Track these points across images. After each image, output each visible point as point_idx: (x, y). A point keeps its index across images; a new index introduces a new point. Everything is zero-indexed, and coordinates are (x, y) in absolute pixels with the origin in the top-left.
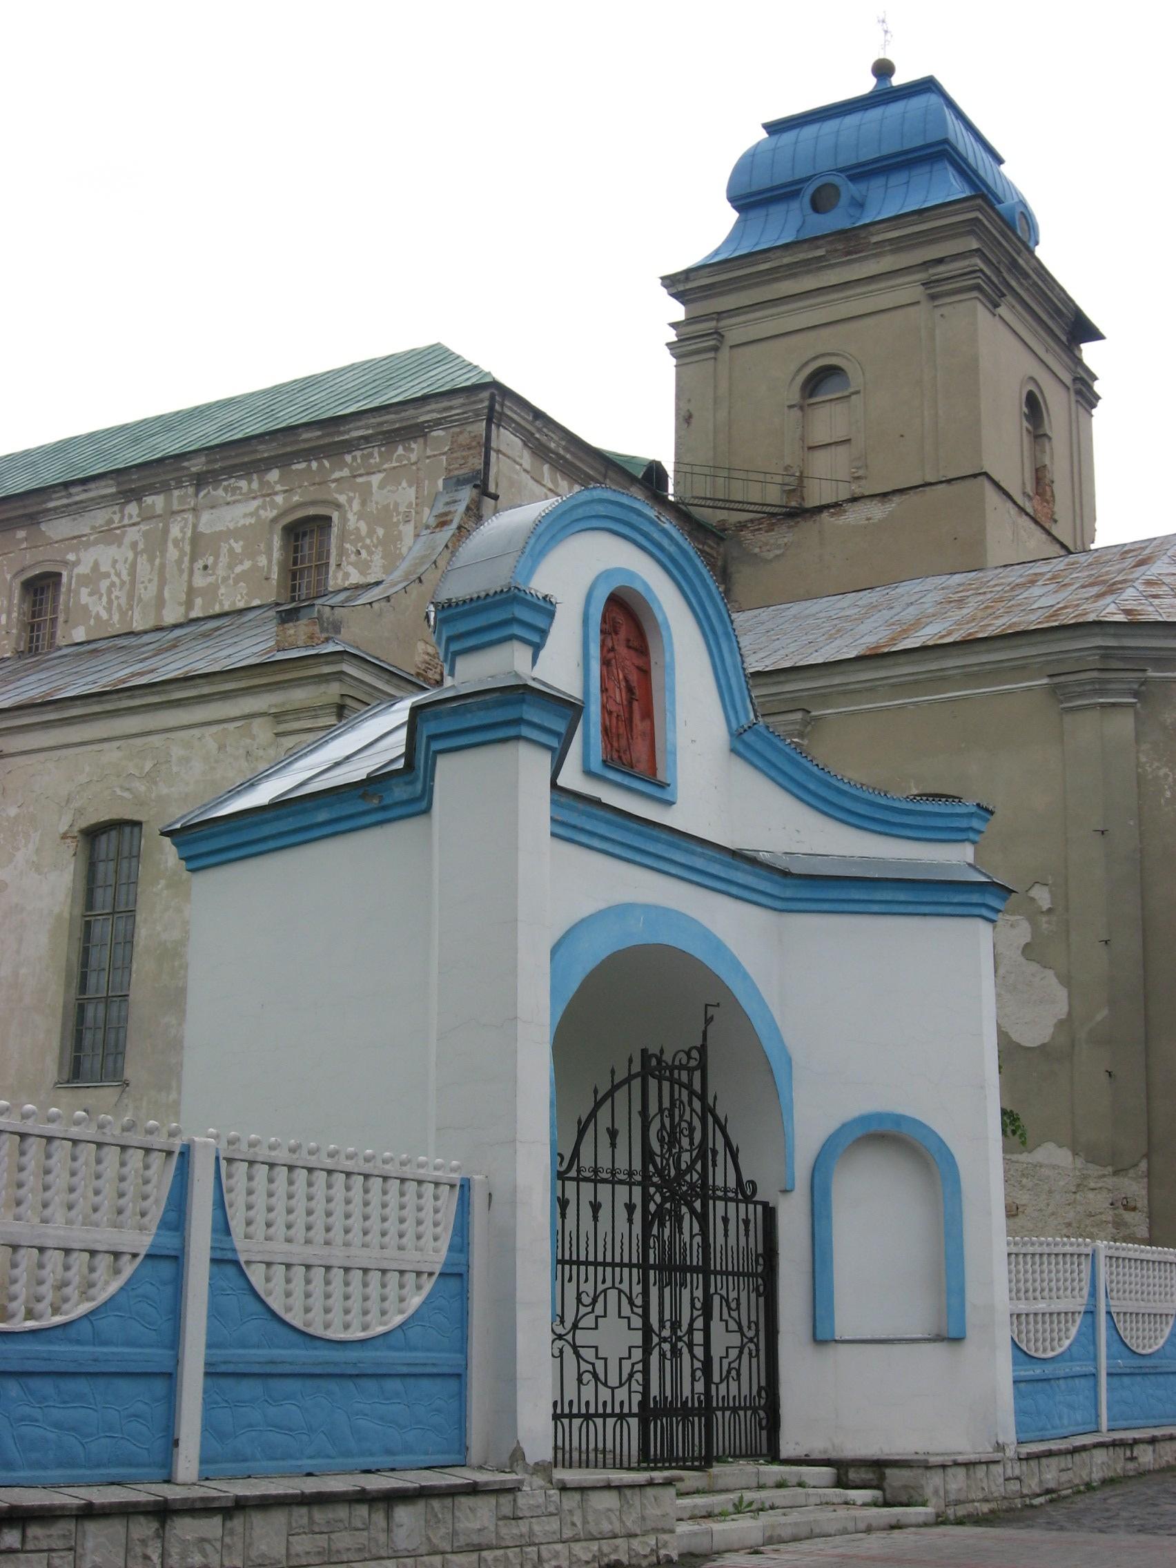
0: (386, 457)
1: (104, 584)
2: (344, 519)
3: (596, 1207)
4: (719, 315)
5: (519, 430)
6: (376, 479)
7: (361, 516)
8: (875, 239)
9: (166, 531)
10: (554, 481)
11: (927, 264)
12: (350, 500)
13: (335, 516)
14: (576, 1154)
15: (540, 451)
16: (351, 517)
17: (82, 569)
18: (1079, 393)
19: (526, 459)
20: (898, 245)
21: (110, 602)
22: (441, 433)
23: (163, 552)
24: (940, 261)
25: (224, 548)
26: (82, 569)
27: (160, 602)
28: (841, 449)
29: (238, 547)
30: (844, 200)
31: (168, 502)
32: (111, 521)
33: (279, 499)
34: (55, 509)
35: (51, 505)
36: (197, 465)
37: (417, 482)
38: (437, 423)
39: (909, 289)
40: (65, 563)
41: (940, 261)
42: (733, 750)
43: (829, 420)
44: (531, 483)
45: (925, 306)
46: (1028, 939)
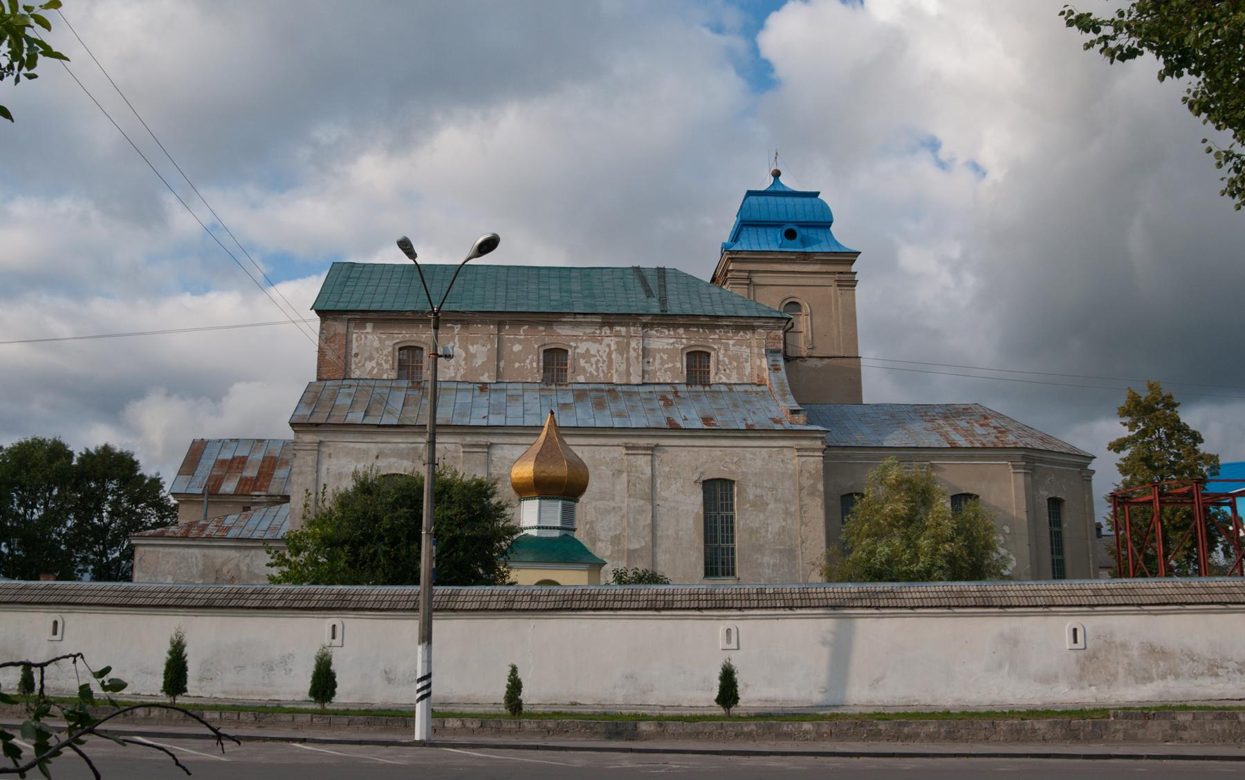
1: (593, 360)
6: (731, 342)
9: (628, 344)
13: (713, 353)
20: (824, 262)
23: (628, 352)
25: (658, 356)
27: (628, 374)
29: (665, 357)
31: (628, 332)
36: (645, 320)
38: (761, 327)
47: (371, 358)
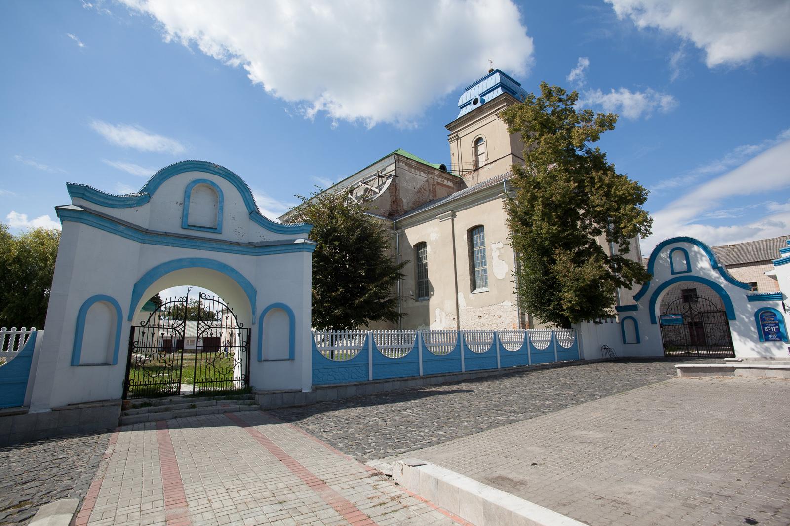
3: (144, 333)
4: (457, 132)
5: (404, 162)
10: (415, 172)
11: (496, 111)
14: (149, 321)
15: (410, 166)
19: (407, 168)
28: (484, 154)
41: (499, 109)
42: (250, 219)
43: (481, 149)
44: (408, 173)
46: (499, 255)
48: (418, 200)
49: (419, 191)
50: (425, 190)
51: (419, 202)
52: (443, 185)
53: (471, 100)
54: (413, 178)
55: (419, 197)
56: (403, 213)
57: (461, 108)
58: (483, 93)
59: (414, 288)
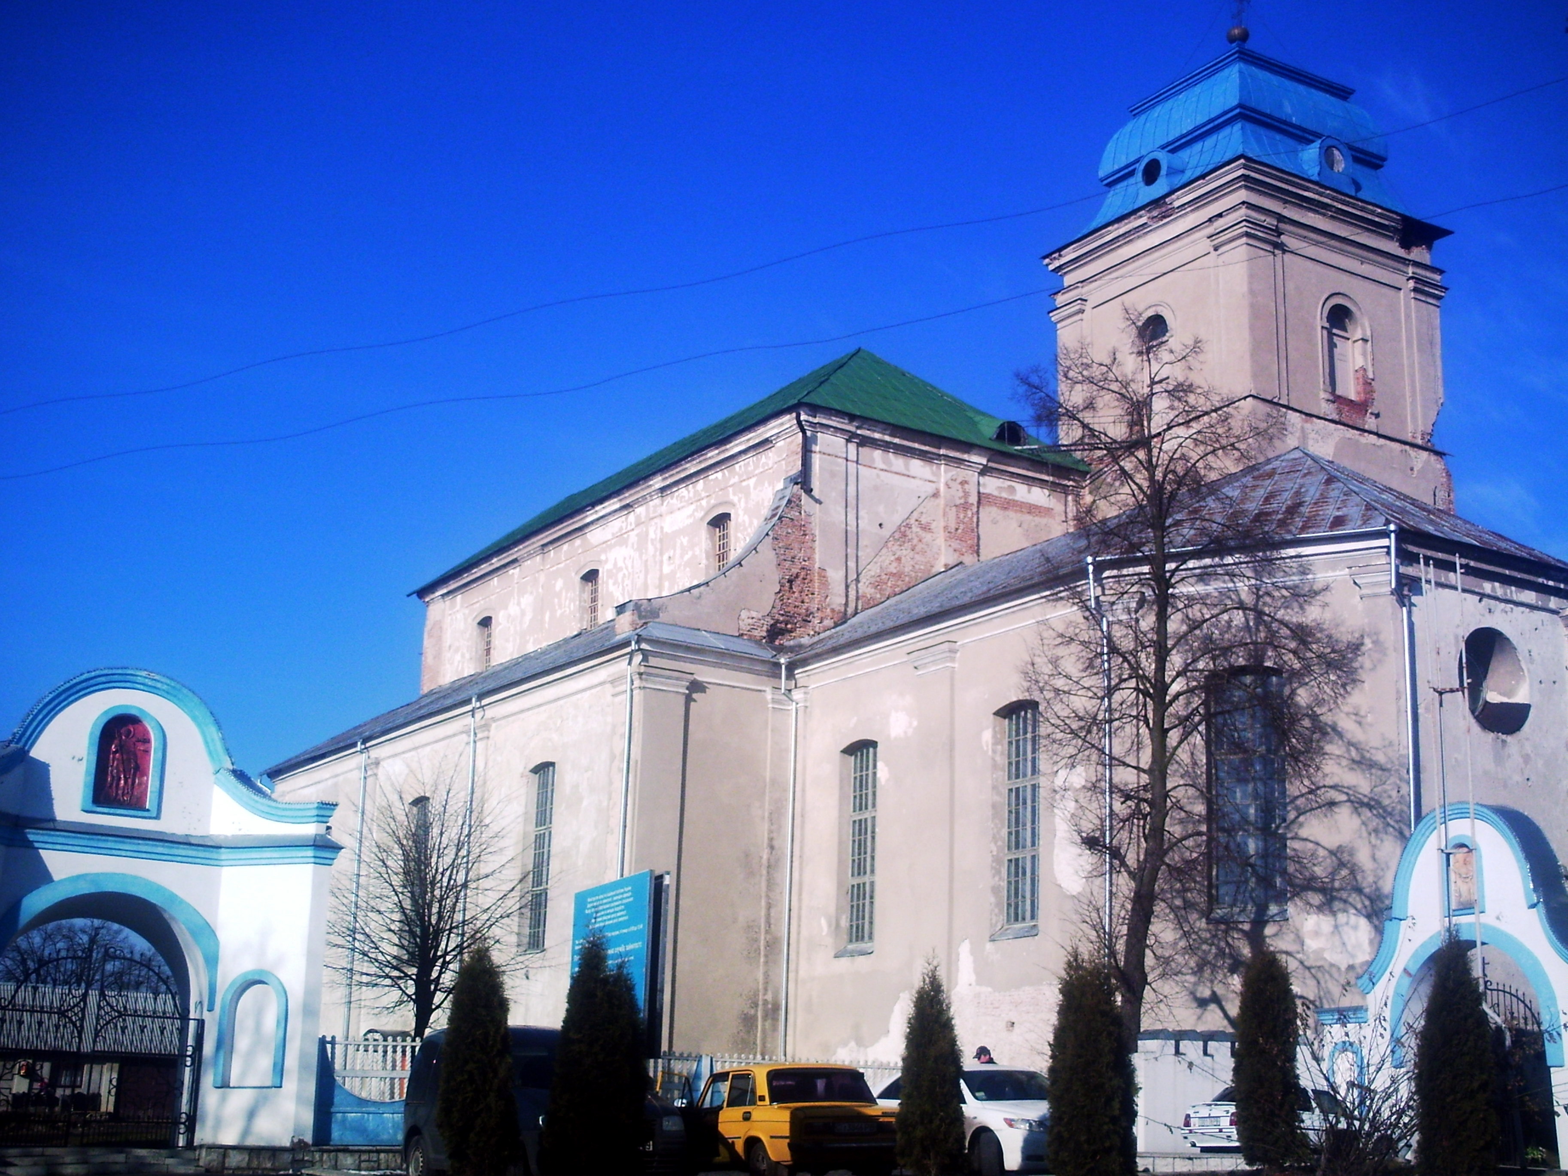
0: (756, 467)
1: (620, 575)
2: (737, 515)
6: (752, 482)
7: (746, 511)
8: (1176, 204)
10: (887, 462)
12: (739, 501)
16: (741, 512)
17: (609, 566)
18: (1415, 290)
21: (623, 589)
22: (782, 443)
24: (1220, 215)
26: (609, 566)
29: (685, 541)
30: (1163, 171)
32: (621, 529)
33: (704, 503)
34: (592, 523)
35: (588, 520)
37: (771, 483)
39: (1200, 243)
40: (600, 561)
41: (1220, 215)
45: (1213, 254)
47: (457, 650)
48: (893, 569)
49: (902, 534)
50: (926, 528)
51: (898, 575)
52: (1007, 505)
53: (1137, 161)
54: (876, 488)
55: (899, 559)
56: (828, 623)
57: (1110, 185)
58: (1183, 136)
59: (832, 910)
